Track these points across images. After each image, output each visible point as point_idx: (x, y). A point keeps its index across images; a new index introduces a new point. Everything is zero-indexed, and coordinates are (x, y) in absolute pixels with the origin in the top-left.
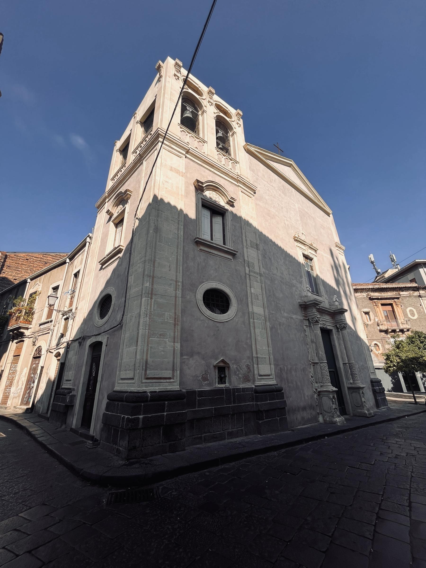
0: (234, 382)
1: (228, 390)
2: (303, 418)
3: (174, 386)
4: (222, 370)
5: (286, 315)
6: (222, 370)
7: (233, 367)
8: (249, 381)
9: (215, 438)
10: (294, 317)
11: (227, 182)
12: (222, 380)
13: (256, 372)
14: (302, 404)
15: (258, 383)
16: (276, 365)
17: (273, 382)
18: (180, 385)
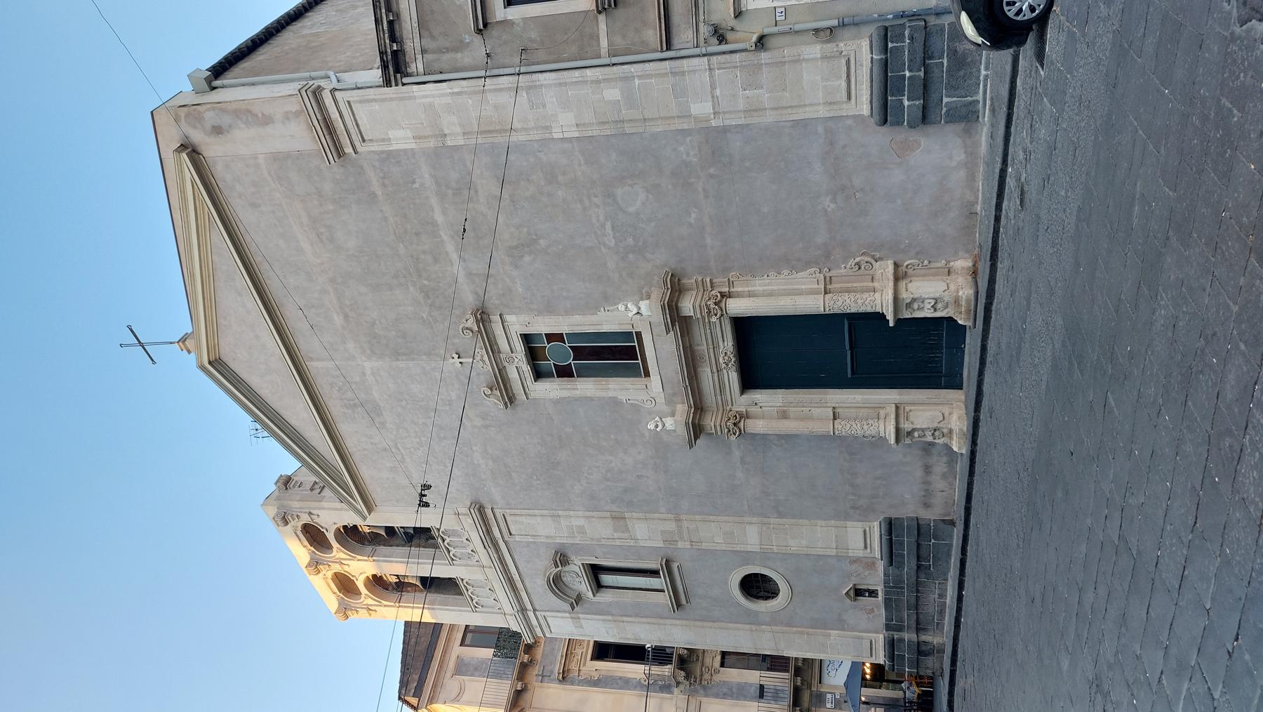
0: (876, 579)
1: (886, 593)
2: (944, 476)
3: (880, 639)
4: (858, 592)
5: (740, 474)
6: (858, 592)
7: (854, 580)
8: (874, 564)
9: (942, 612)
10: (737, 454)
11: (516, 557)
12: (873, 593)
13: (861, 554)
14: (919, 473)
15: (877, 554)
16: (847, 517)
17: (876, 524)
18: (877, 632)
